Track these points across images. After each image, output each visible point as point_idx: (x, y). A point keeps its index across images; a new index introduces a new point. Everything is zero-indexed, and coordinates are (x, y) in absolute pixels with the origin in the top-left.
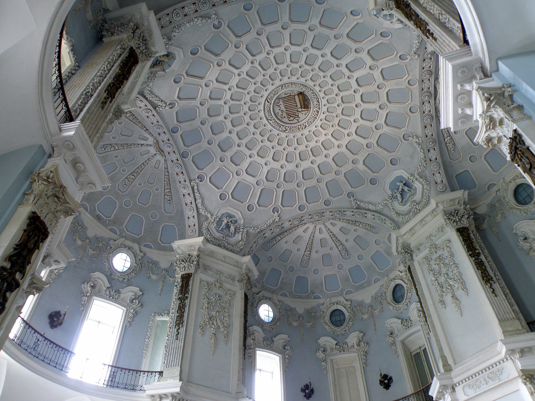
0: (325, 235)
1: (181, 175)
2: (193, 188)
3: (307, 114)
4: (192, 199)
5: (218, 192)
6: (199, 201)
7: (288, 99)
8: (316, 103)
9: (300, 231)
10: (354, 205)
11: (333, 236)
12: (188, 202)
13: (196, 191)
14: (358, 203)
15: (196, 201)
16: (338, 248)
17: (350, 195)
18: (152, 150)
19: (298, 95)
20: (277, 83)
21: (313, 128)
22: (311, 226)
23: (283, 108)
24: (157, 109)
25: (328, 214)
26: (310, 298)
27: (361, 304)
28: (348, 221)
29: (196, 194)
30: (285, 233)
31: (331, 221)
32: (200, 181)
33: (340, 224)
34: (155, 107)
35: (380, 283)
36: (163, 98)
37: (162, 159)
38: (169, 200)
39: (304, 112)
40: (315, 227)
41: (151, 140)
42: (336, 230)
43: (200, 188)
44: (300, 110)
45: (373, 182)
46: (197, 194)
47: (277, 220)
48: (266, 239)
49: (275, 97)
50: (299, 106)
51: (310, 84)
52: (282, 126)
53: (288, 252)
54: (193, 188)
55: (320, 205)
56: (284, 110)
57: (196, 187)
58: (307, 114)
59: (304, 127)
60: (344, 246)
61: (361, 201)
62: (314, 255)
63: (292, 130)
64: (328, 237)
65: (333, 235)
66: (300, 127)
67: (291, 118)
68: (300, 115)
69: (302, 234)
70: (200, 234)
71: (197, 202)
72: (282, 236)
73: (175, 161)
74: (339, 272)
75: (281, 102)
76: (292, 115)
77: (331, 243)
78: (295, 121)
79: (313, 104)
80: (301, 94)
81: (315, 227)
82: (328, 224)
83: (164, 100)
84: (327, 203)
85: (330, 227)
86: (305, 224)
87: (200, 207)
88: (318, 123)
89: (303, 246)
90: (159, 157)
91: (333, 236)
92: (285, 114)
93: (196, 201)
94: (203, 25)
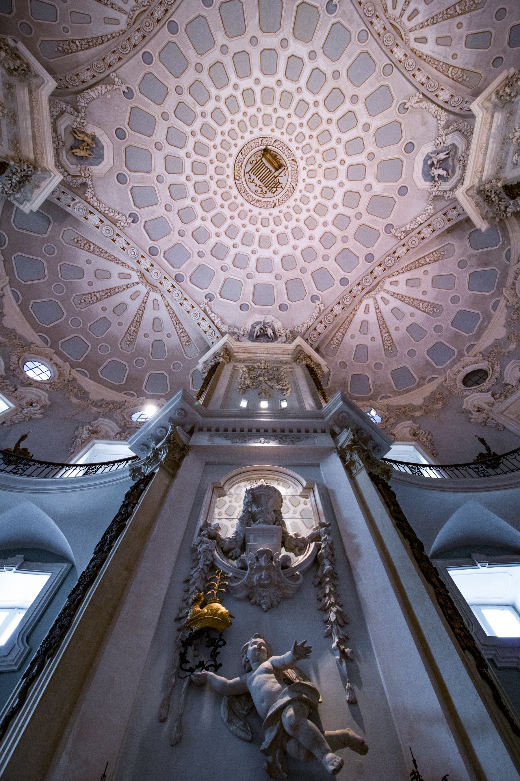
0: (394, 303)
1: (185, 303)
2: (205, 311)
3: (286, 173)
4: (208, 322)
5: (236, 305)
6: (217, 321)
7: (256, 168)
8: (286, 151)
9: (360, 315)
10: (399, 235)
11: (402, 298)
12: (206, 328)
13: (210, 313)
14: (403, 229)
15: (214, 323)
16: (419, 309)
17: (389, 228)
18: (142, 288)
19: (263, 155)
20: (235, 151)
21: (301, 185)
22: (369, 301)
23: (259, 183)
24: (118, 225)
25: (378, 271)
26: (424, 384)
27: (498, 344)
28: (409, 268)
29: (211, 316)
30: (344, 325)
31: (388, 280)
32: (210, 301)
33: (402, 278)
34: (114, 222)
35: (503, 303)
36: (118, 209)
37: (158, 296)
38: (187, 342)
39: (282, 174)
40: (375, 299)
41: (135, 277)
42: (402, 289)
43: (213, 309)
44: (276, 174)
45: (403, 191)
46: (212, 316)
47: (323, 308)
48: (322, 336)
49: (243, 171)
50: (273, 170)
51: (266, 131)
52: (268, 203)
53: (361, 348)
54: (205, 311)
55: (363, 267)
56: (261, 184)
57: (207, 308)
58: (286, 173)
59: (292, 189)
60: (424, 302)
61: (404, 226)
62: (395, 335)
63: (282, 202)
64: (397, 303)
65: (402, 296)
66: (287, 192)
67: (274, 189)
68: (281, 180)
69: (365, 317)
70: (223, 334)
71: (216, 323)
72: (341, 331)
73: (171, 289)
74: (440, 336)
75: (253, 177)
76: (272, 185)
77: (407, 309)
78: (279, 190)
79: (285, 159)
80: (266, 150)
81: (375, 299)
82: (387, 286)
83: (121, 211)
84: (369, 258)
85: (392, 289)
86: (361, 302)
87: (222, 326)
88: (303, 174)
89: (374, 330)
90: (153, 295)
91: (402, 298)
92: (264, 189)
93: (214, 323)
94: (112, 96)
